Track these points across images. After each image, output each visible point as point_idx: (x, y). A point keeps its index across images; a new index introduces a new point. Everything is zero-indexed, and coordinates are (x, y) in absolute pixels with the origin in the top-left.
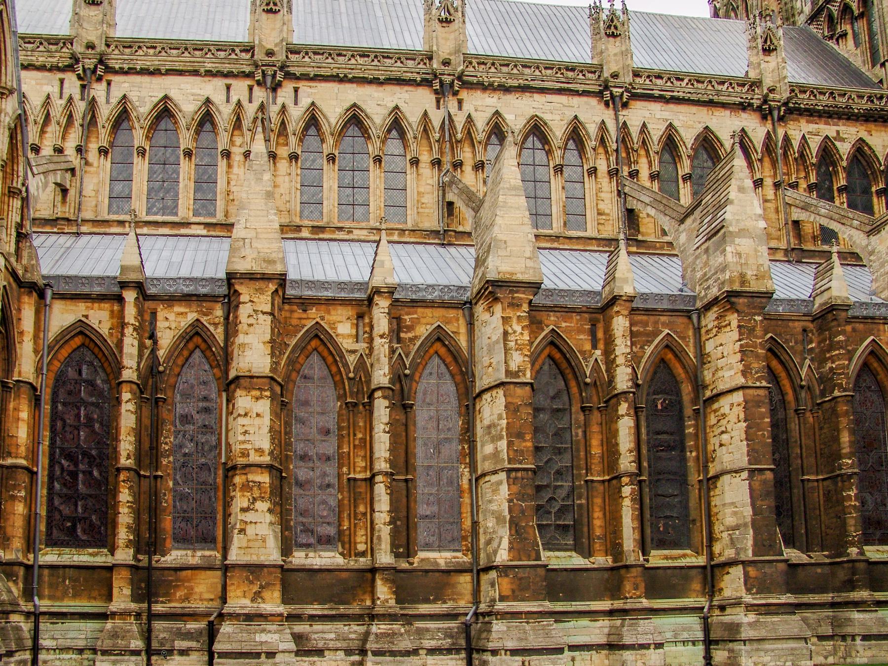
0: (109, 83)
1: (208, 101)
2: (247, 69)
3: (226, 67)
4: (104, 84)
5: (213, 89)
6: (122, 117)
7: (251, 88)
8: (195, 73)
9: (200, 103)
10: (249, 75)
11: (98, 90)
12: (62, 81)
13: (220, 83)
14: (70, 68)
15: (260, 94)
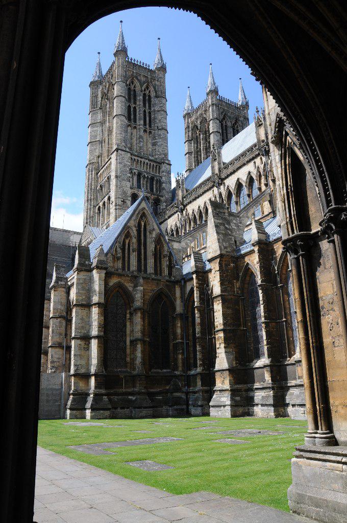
0: (224, 183)
1: (249, 173)
2: (257, 153)
3: (251, 157)
4: (223, 184)
5: (250, 167)
6: (230, 195)
7: (261, 159)
8: (244, 165)
9: (246, 176)
10: (258, 155)
11: (222, 187)
12: (213, 191)
13: (252, 163)
14: (213, 186)
15: (264, 159)
